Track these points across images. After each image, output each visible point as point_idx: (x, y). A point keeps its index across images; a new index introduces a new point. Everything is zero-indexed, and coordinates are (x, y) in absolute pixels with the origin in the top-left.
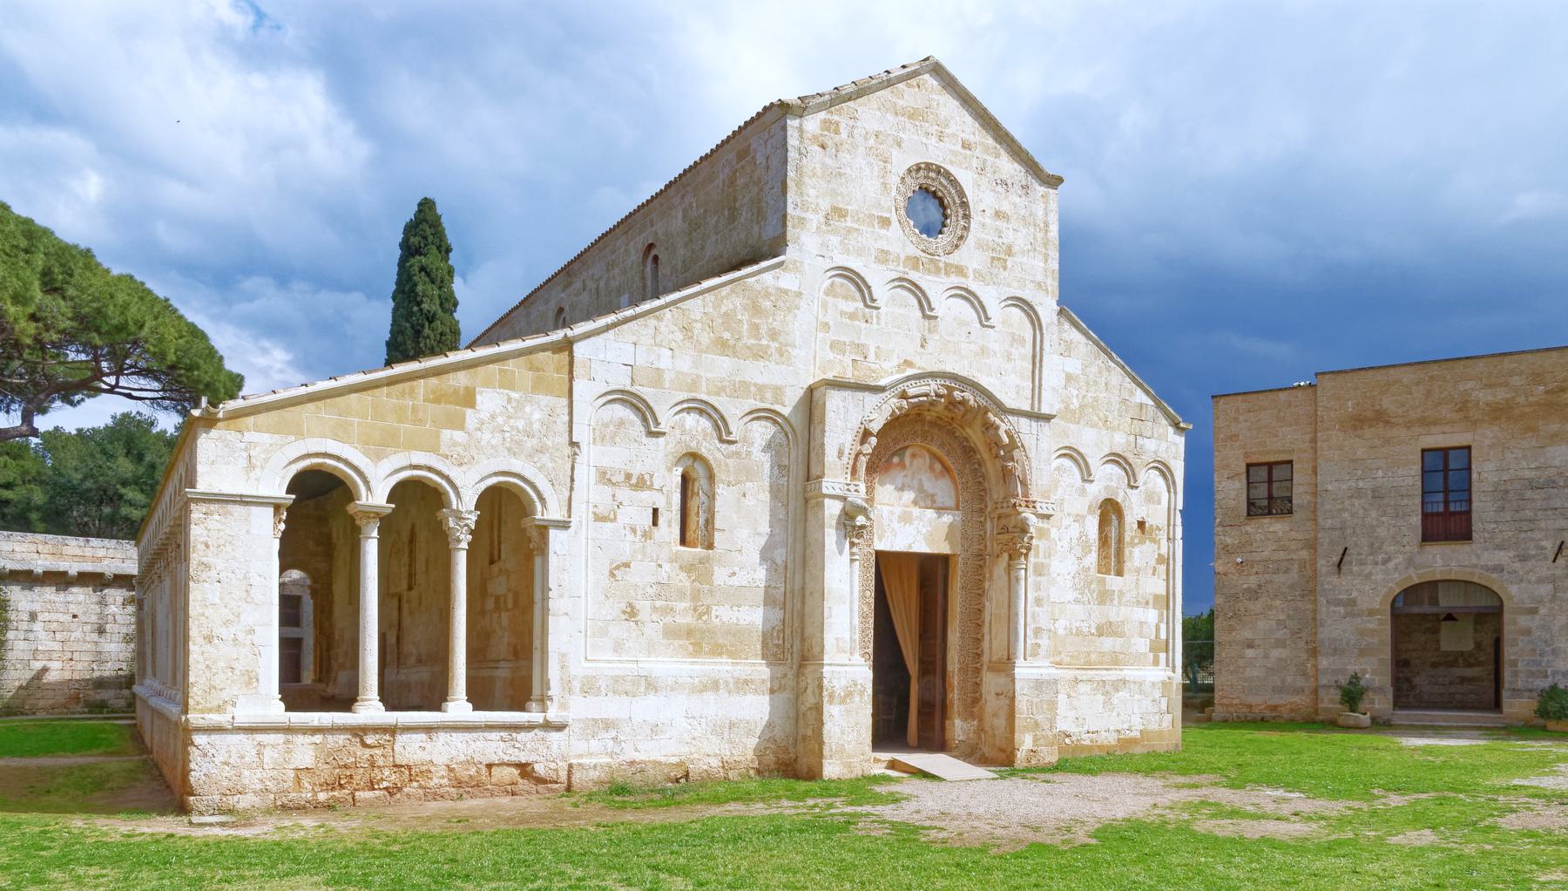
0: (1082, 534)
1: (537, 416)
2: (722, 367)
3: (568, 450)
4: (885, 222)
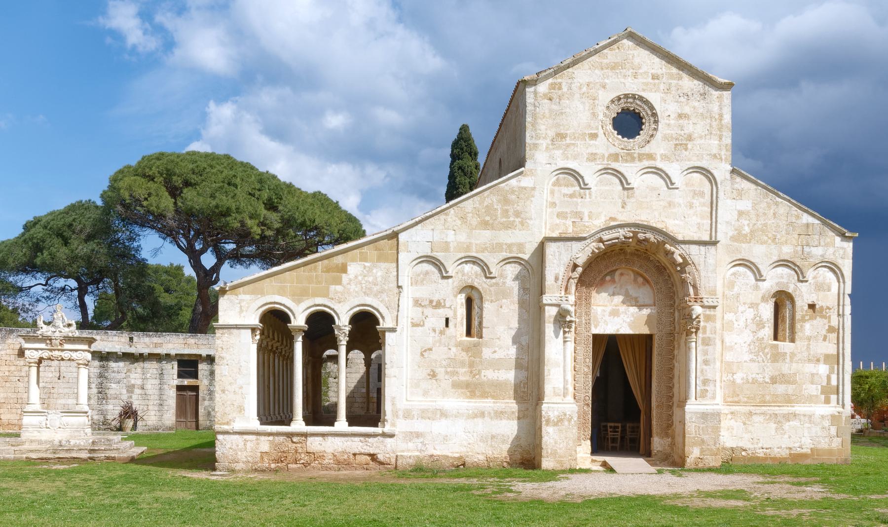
1: (379, 274)
2: (485, 236)
3: (396, 290)
4: (594, 136)
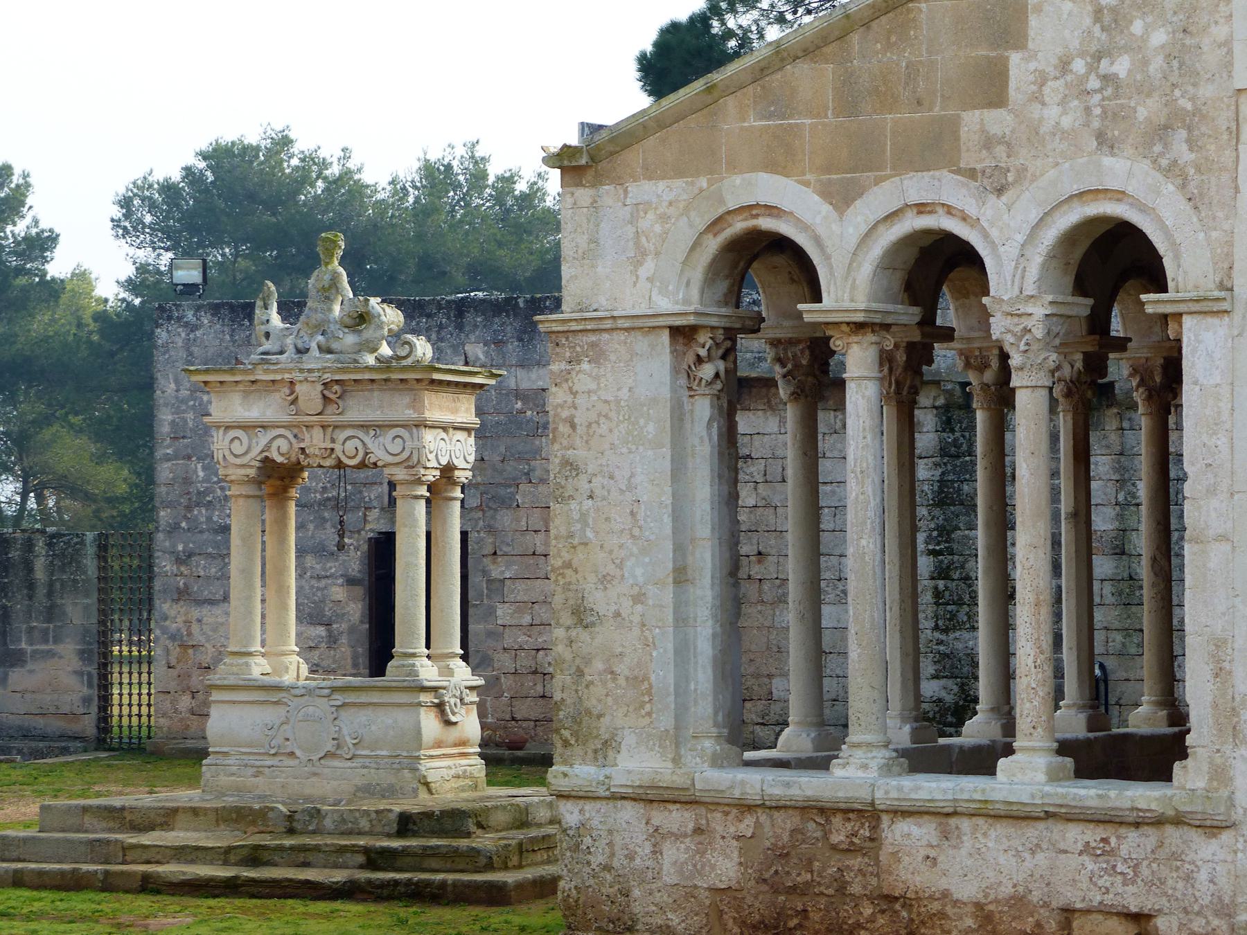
1: (1159, 37)
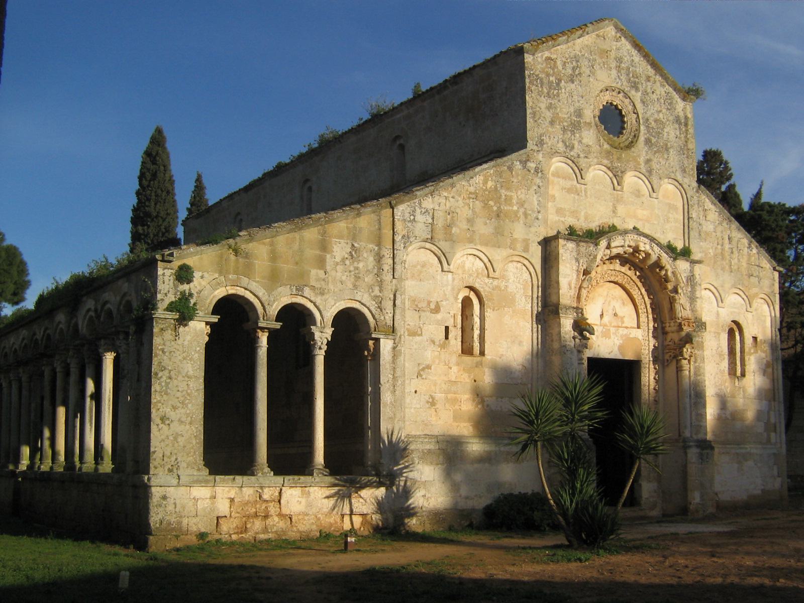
0: (719, 347)
